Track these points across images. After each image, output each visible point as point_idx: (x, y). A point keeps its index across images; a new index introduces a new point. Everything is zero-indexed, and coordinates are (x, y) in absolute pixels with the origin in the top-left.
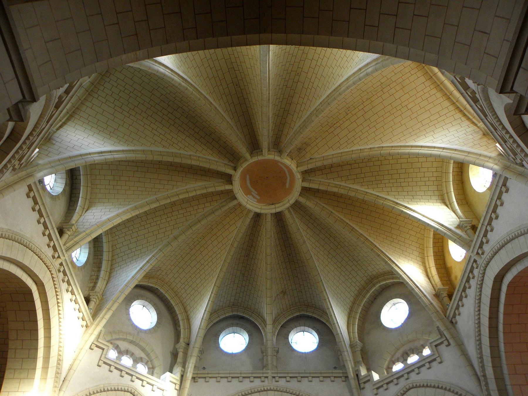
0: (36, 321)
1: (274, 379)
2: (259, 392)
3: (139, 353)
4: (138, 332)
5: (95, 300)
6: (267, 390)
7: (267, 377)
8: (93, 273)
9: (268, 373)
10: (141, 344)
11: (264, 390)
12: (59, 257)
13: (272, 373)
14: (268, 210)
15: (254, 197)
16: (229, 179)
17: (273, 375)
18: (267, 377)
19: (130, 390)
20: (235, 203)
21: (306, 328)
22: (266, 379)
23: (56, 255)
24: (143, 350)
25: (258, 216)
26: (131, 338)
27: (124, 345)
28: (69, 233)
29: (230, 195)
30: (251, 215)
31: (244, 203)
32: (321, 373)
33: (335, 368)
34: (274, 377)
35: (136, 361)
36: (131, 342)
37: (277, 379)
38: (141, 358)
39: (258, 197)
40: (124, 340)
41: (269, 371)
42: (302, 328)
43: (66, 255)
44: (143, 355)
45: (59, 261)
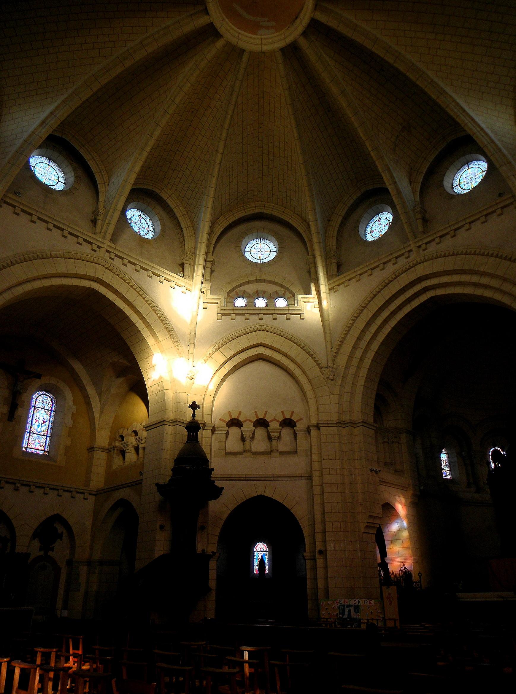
0: (120, 311)
1: (421, 250)
2: (406, 271)
3: (270, 288)
4: (260, 269)
5: (187, 262)
6: (414, 266)
7: (411, 251)
8: (179, 235)
9: (410, 245)
10: (268, 278)
11: (411, 267)
12: (99, 247)
13: (415, 243)
14: (293, 33)
15: (268, 28)
16: (211, 32)
17: (418, 244)
18: (411, 251)
19: (259, 328)
20: (246, 56)
21: (468, 157)
22: (411, 253)
23: (95, 247)
24: (274, 283)
25: (291, 51)
26: (253, 278)
27: (250, 288)
28: (100, 218)
29: (234, 52)
30: (279, 57)
31: (258, 48)
32: (480, 212)
33: (500, 195)
34: (420, 247)
35: (271, 298)
36: (257, 281)
37: (423, 246)
38: (276, 292)
39: (273, 24)
40: (248, 282)
41: (411, 242)
42: (463, 159)
43: (105, 242)
44: (277, 288)
45: (103, 250)
